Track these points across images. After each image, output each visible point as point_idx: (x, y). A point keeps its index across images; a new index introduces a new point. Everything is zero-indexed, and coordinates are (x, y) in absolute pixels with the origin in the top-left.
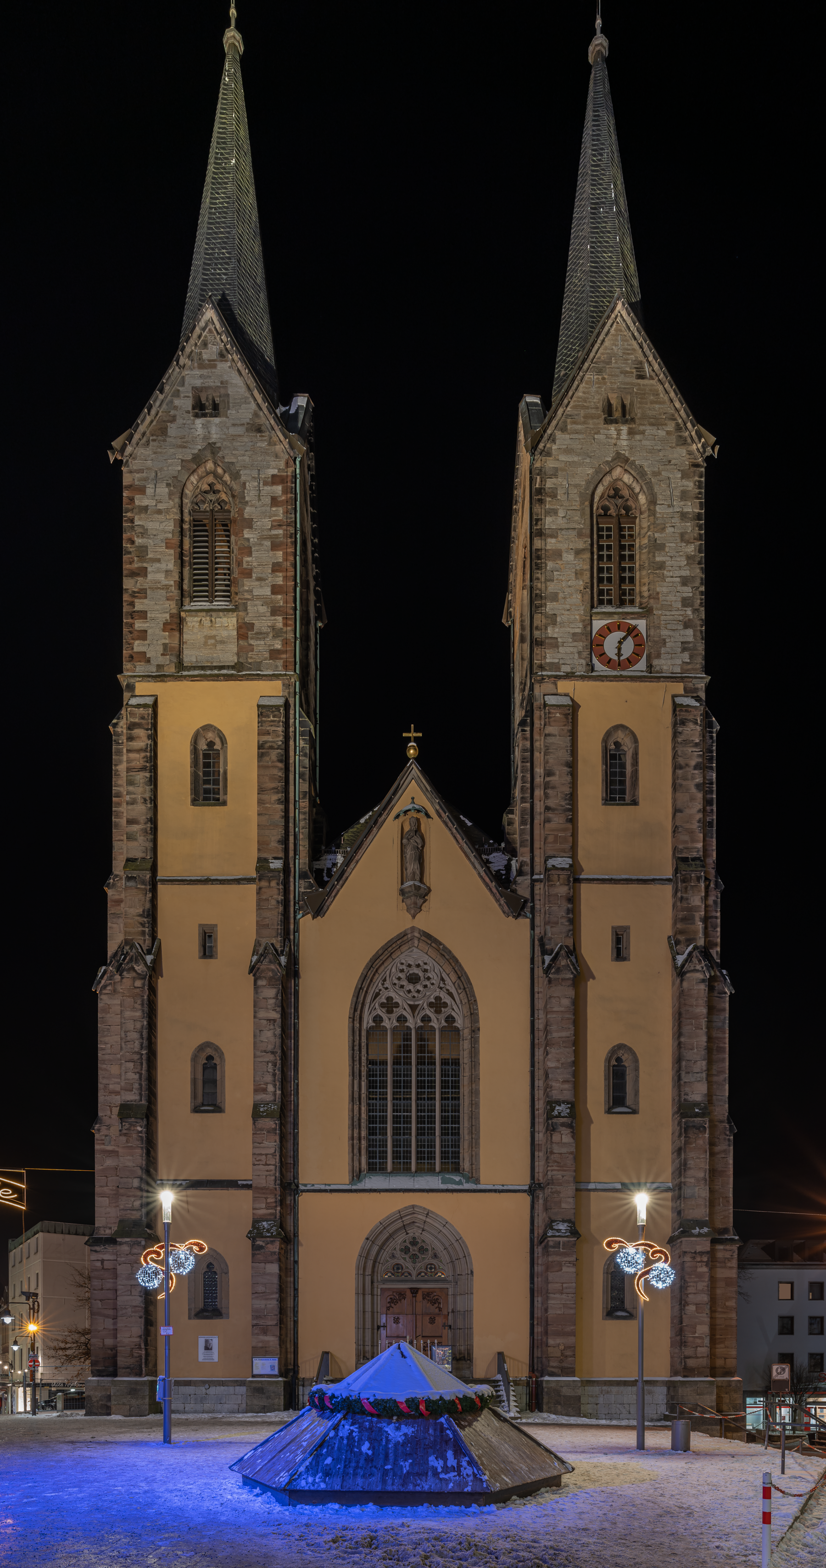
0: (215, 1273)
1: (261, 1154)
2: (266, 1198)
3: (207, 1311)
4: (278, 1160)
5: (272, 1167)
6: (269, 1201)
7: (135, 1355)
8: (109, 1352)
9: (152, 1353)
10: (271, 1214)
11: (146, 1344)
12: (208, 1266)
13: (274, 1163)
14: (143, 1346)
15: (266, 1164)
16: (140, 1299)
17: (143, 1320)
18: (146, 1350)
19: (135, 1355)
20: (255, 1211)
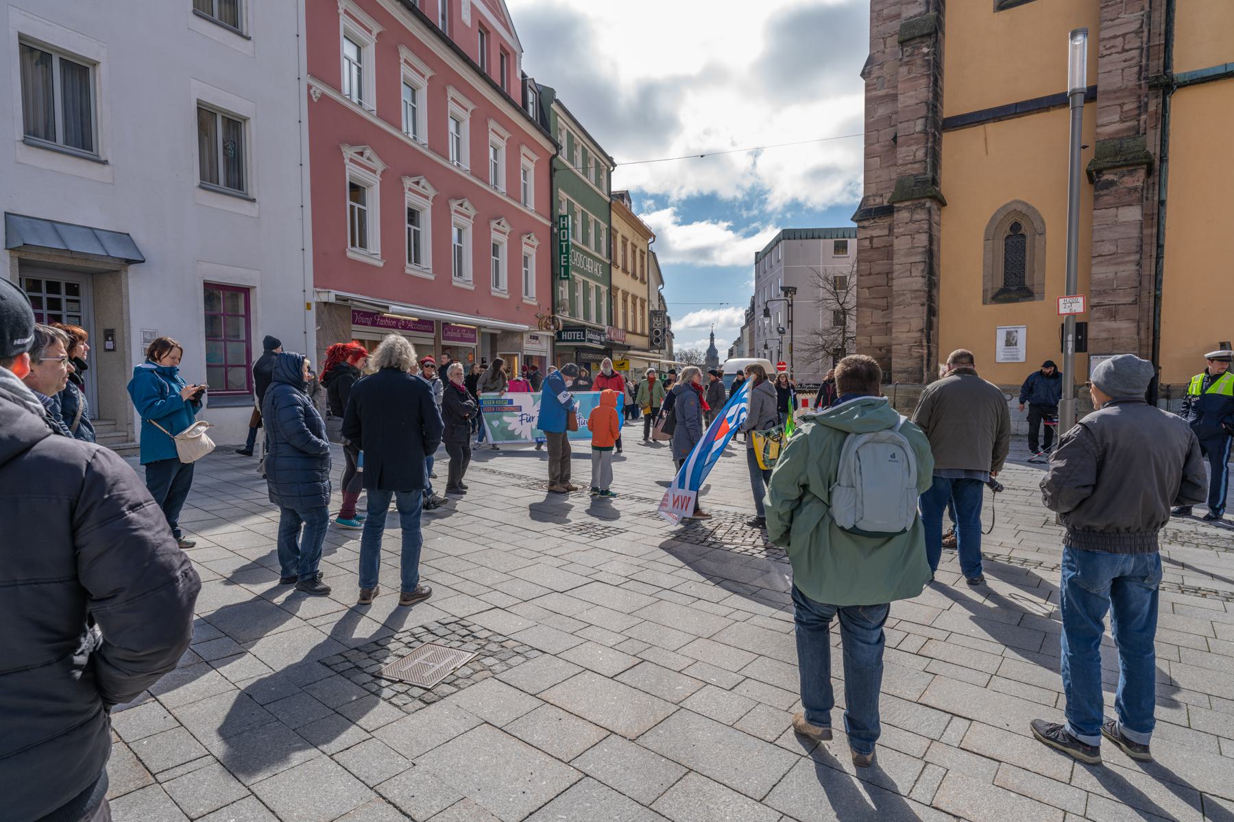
0: (1023, 236)
1: (1115, 37)
2: (1121, 105)
3: (1010, 291)
4: (1145, 39)
5: (1135, 53)
6: (1126, 108)
7: (915, 354)
9: (933, 350)
10: (1129, 129)
11: (929, 341)
12: (1011, 229)
13: (1138, 44)
14: (925, 343)
15: (1124, 50)
16: (922, 280)
17: (926, 308)
18: (929, 347)
20: (1099, 130)
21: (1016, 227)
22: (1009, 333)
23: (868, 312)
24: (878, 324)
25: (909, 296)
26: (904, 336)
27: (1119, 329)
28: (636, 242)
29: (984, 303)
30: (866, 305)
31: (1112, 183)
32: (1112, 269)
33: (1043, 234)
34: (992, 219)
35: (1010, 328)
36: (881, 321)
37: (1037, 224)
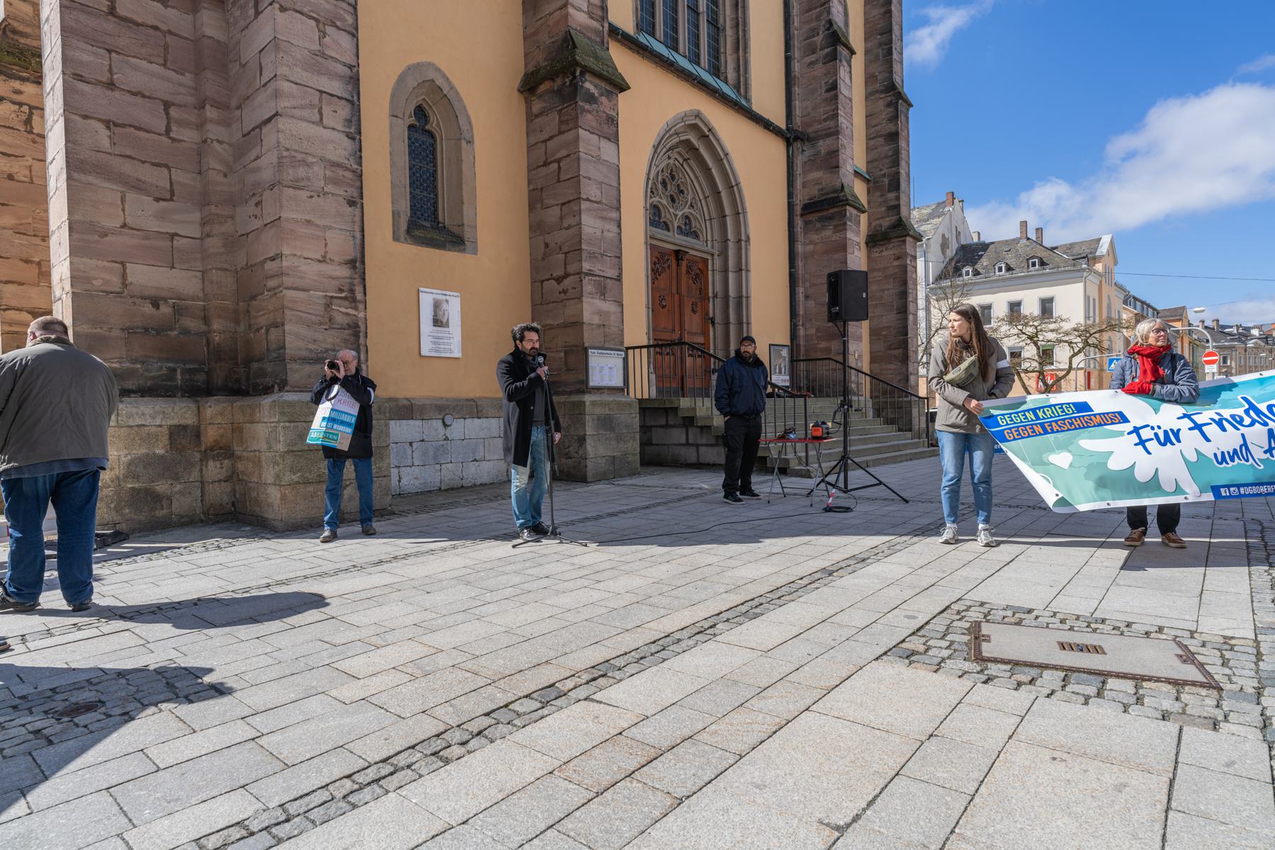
7: (340, 319)
8: (148, 309)
19: (340, 319)
21: (420, 112)
22: (437, 305)
23: (109, 192)
24: (147, 235)
25: (318, 171)
26: (311, 270)
27: (608, 313)
29: (396, 238)
30: (102, 171)
31: (591, 99)
32: (599, 224)
33: (470, 142)
34: (401, 80)
35: (437, 294)
36: (153, 225)
37: (462, 121)
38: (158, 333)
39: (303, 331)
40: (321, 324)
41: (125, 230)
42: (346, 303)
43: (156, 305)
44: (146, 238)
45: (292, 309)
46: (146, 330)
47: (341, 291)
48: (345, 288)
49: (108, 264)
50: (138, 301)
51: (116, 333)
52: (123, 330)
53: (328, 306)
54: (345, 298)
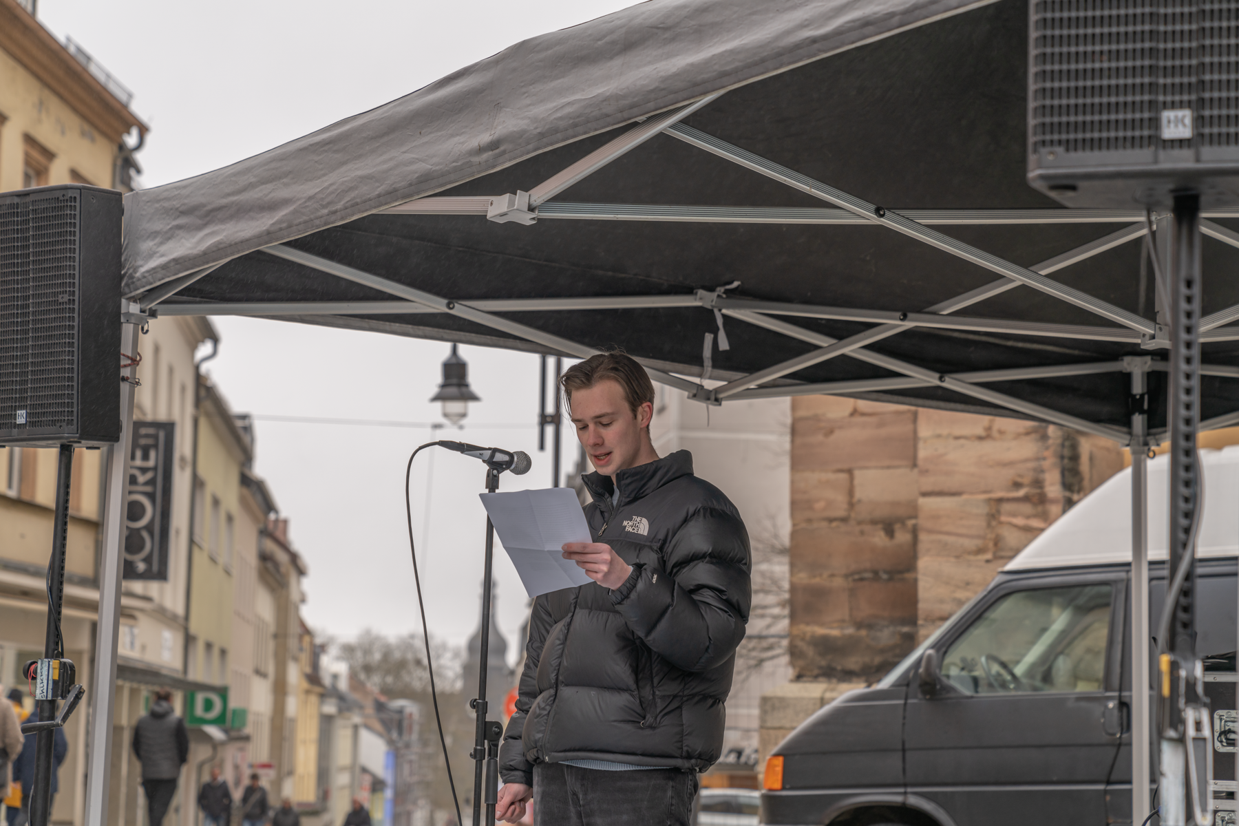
8: (879, 539)
28: (47, 135)
38: (891, 579)
39: (948, 567)
40: (980, 551)
41: (858, 419)
42: (1027, 508)
43: (890, 532)
44: (881, 425)
45: (930, 532)
46: (876, 573)
47: (1017, 485)
48: (1026, 481)
49: (831, 476)
50: (867, 528)
51: (838, 582)
52: (846, 576)
53: (993, 517)
54: (1026, 499)
